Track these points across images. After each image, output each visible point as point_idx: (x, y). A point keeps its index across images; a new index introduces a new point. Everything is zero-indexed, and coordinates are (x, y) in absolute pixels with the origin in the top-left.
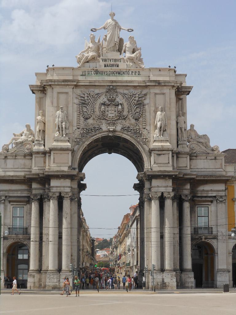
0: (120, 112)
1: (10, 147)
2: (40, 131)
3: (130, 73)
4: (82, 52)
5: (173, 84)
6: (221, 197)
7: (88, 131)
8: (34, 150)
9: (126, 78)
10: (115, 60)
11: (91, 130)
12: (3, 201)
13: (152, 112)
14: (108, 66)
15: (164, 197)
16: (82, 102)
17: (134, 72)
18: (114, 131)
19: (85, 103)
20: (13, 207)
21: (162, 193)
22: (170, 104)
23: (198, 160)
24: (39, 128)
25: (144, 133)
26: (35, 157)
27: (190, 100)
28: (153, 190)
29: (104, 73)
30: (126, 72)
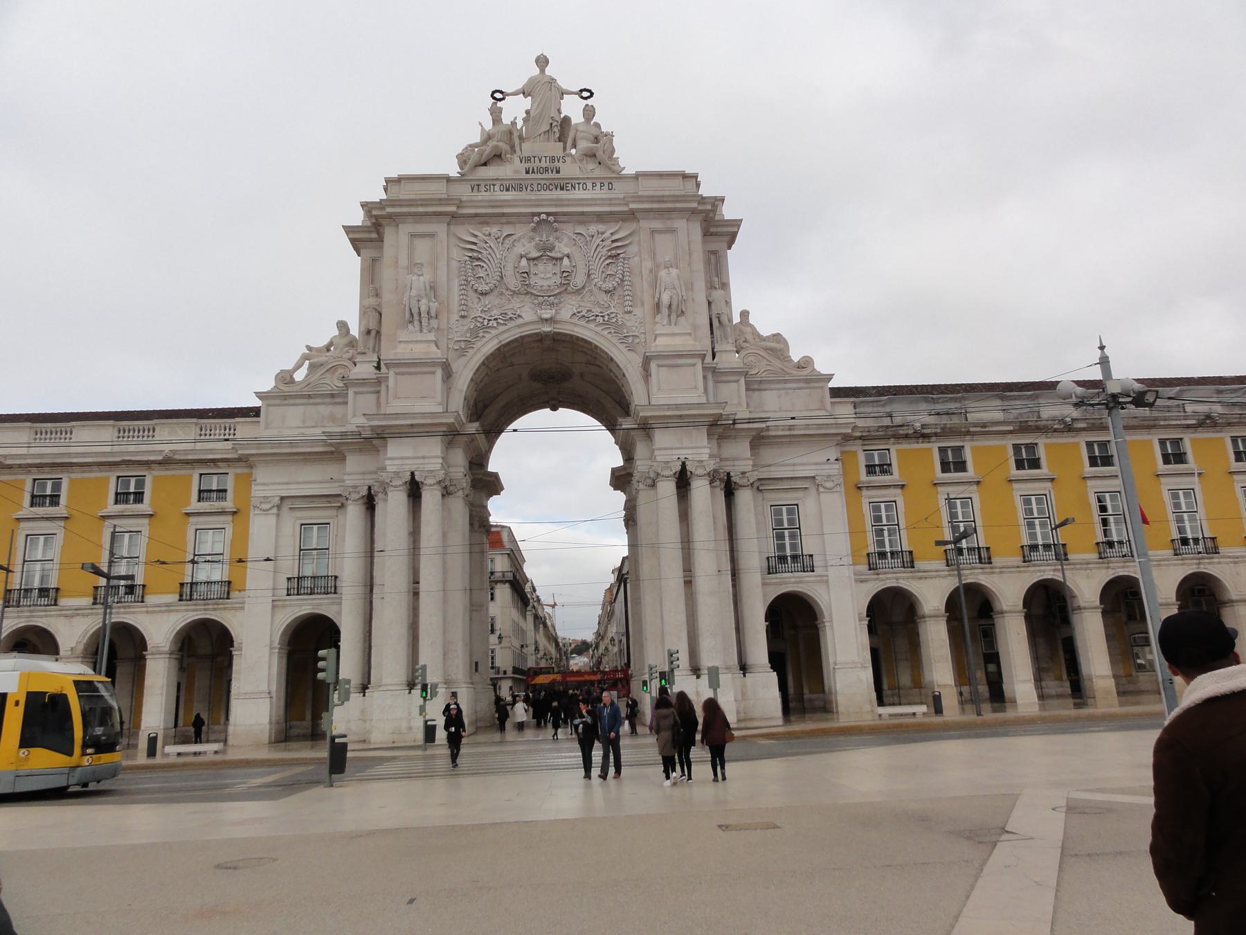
0: (567, 275)
1: (300, 376)
2: (369, 332)
3: (590, 185)
4: (471, 146)
5: (695, 205)
6: (829, 476)
9: (578, 194)
10: (553, 159)
12: (275, 511)
13: (645, 273)
21: (684, 465)
22: (690, 255)
25: (629, 324)
26: (356, 393)
27: (734, 256)
28: (661, 456)
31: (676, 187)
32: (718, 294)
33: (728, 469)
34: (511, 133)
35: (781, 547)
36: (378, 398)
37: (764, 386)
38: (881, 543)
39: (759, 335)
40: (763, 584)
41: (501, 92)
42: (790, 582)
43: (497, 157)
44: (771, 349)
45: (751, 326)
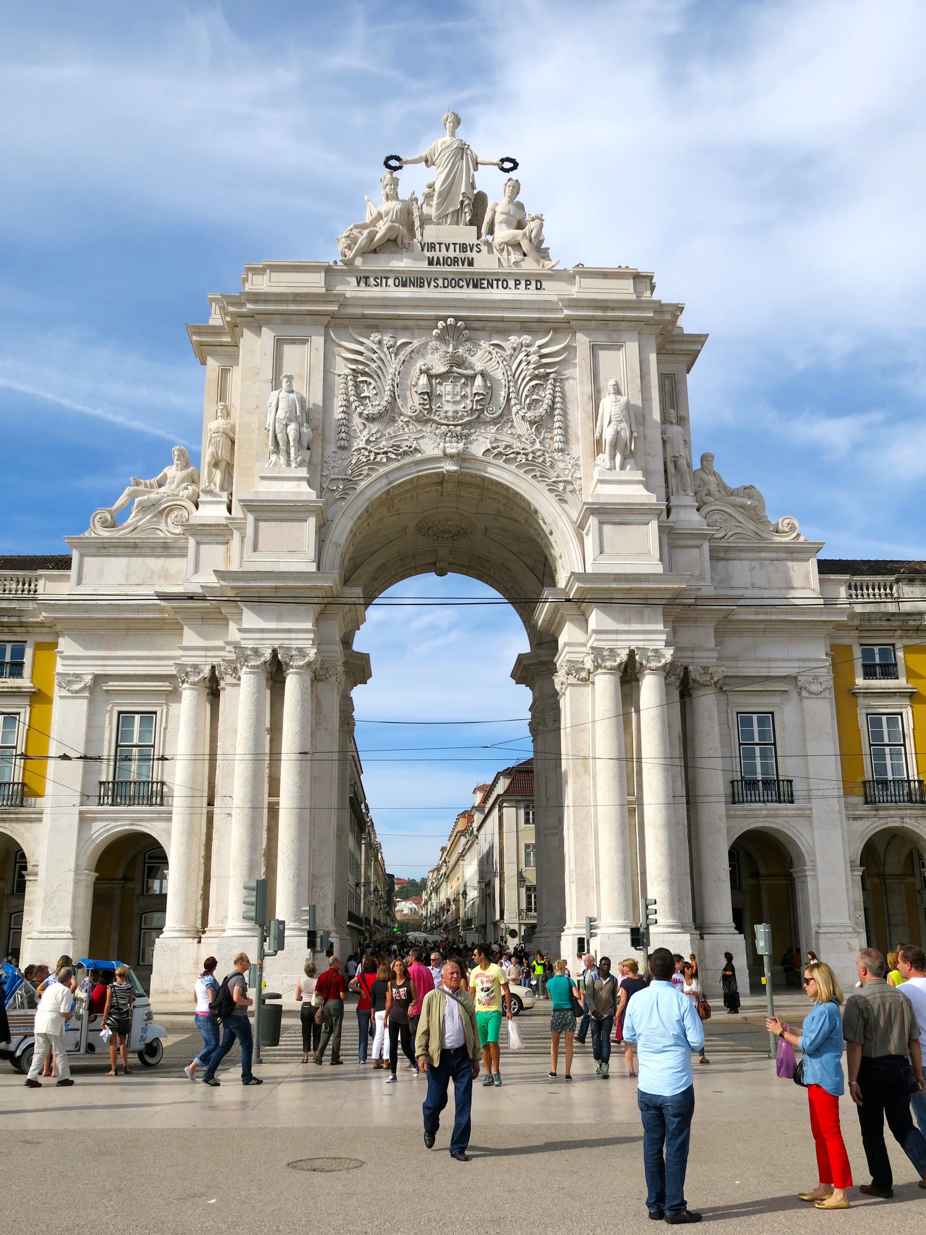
3: (511, 283)
7: (375, 459)
8: (191, 522)
10: (464, 247)
11: (386, 453)
14: (438, 263)
15: (638, 665)
16: (354, 367)
17: (523, 283)
18: (460, 458)
19: (367, 370)
20: (120, 713)
23: (731, 563)
24: (213, 454)
29: (426, 283)
30: (498, 280)
31: (624, 290)
32: (675, 430)
33: (685, 662)
34: (410, 213)
35: (752, 769)
36: (228, 550)
37: (731, 555)
38: (881, 769)
39: (725, 488)
40: (728, 816)
41: (398, 159)
42: (762, 815)
43: (393, 243)
44: (743, 507)
45: (715, 474)
